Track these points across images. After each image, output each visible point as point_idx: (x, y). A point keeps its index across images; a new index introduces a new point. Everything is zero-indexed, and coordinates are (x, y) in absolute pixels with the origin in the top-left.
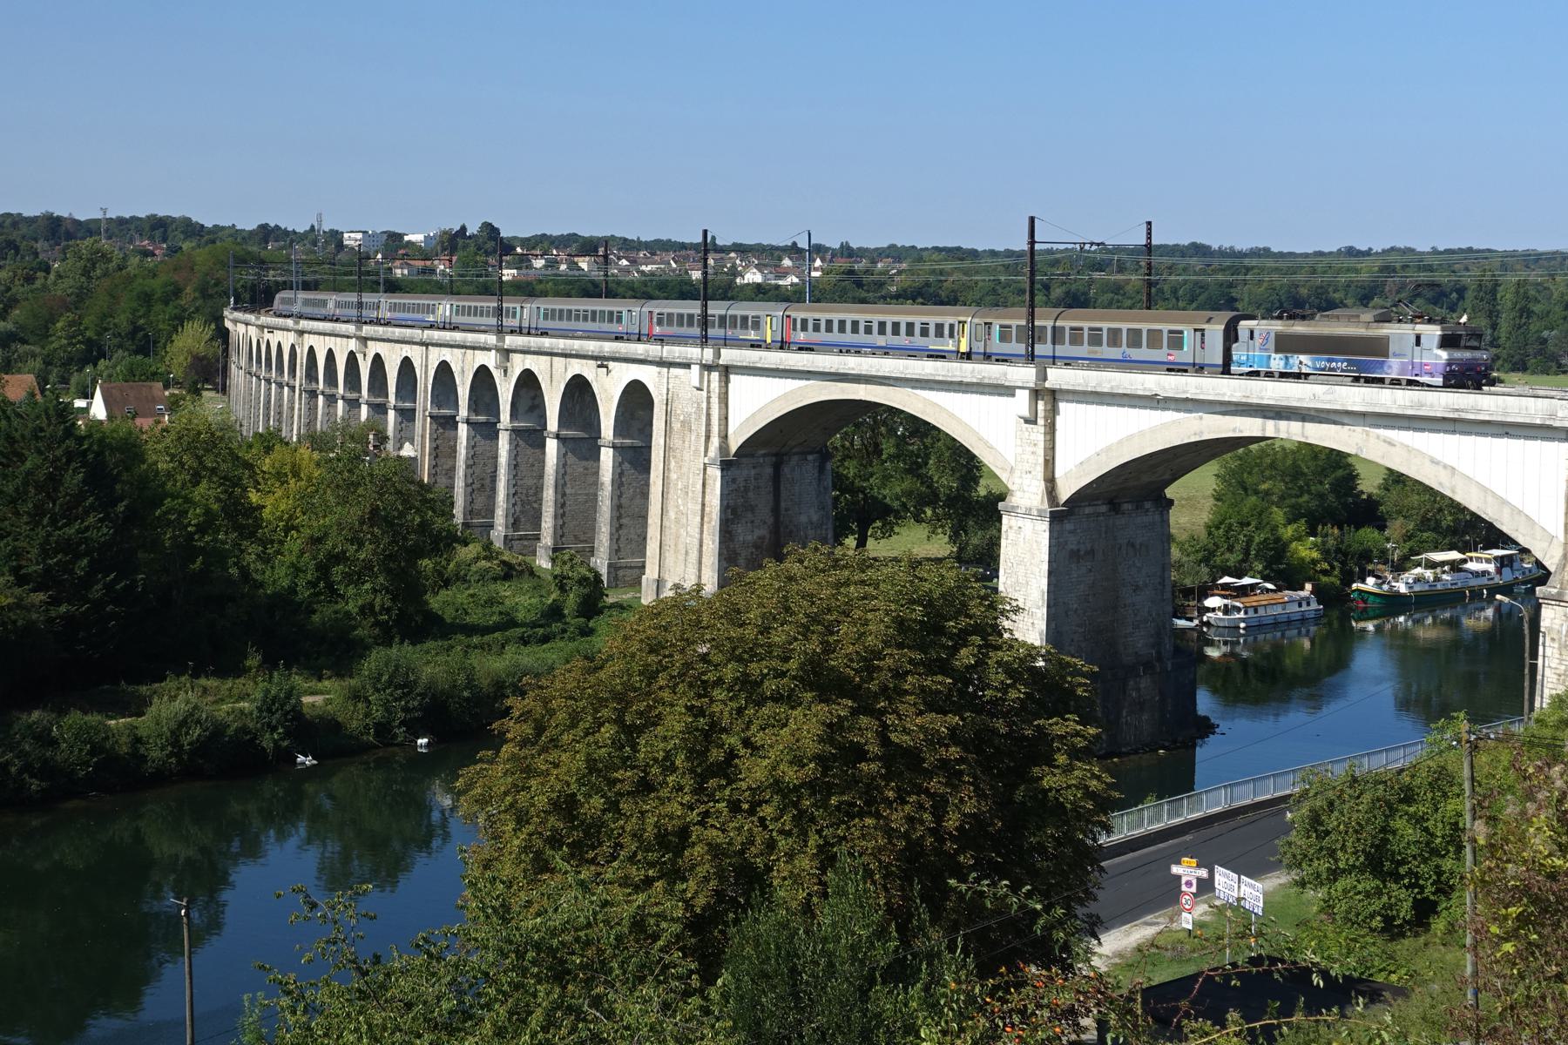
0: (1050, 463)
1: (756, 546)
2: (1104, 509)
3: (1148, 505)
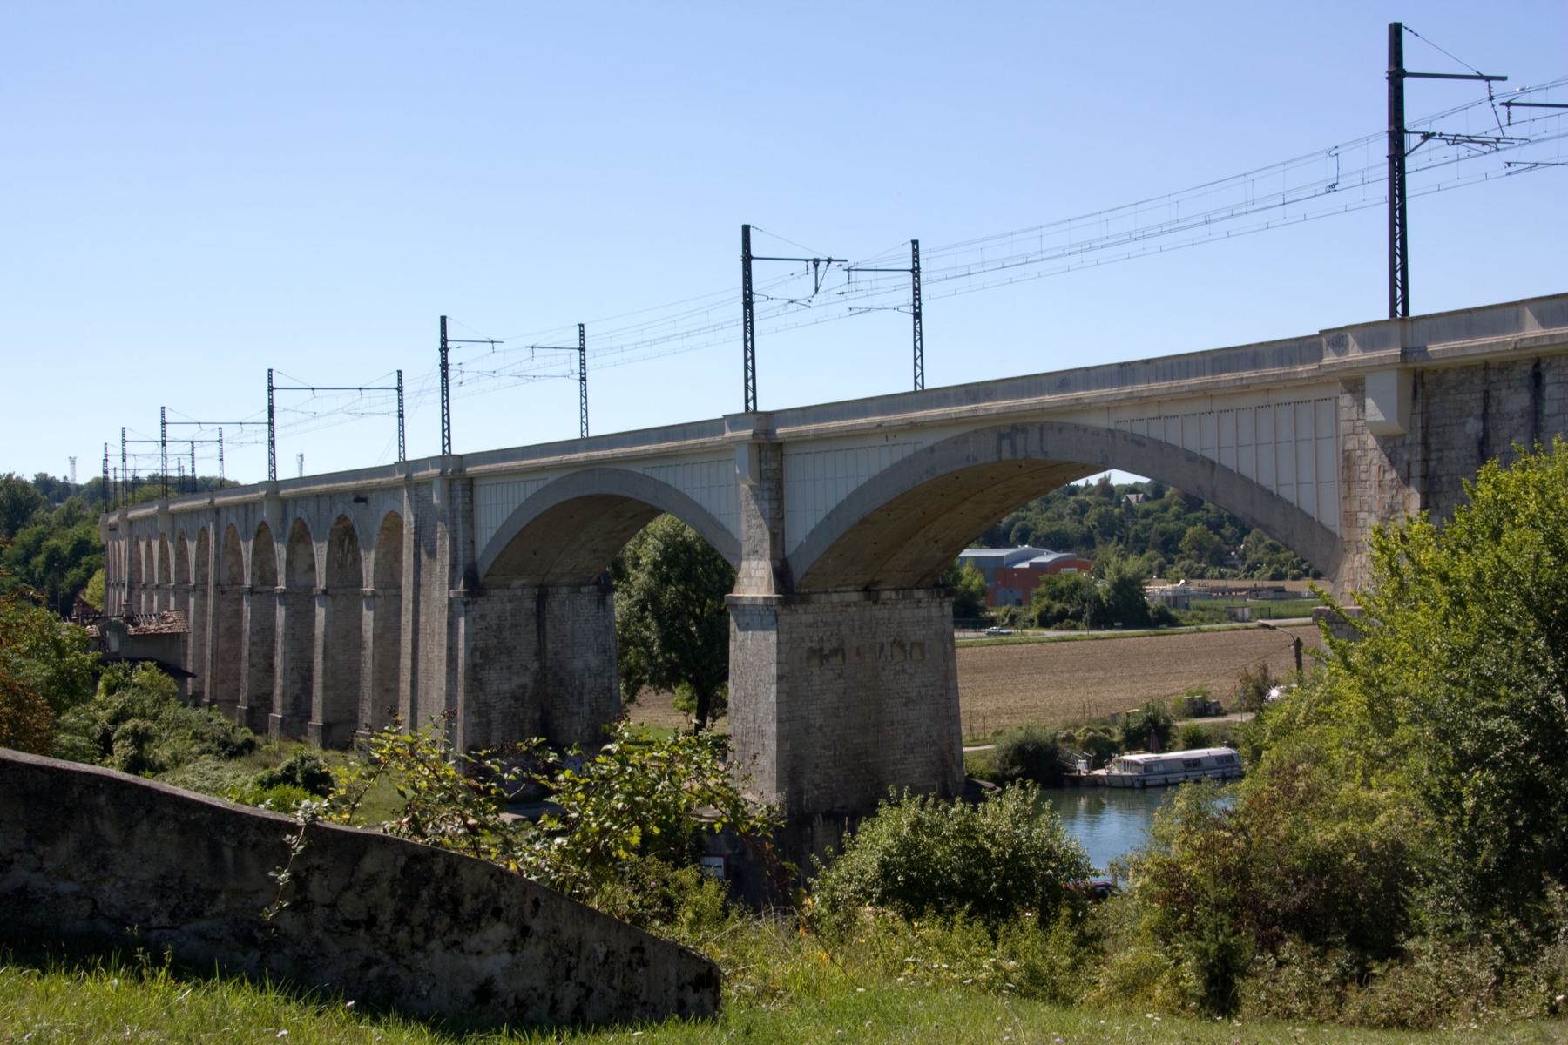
0: (778, 538)
2: (855, 597)
3: (919, 594)
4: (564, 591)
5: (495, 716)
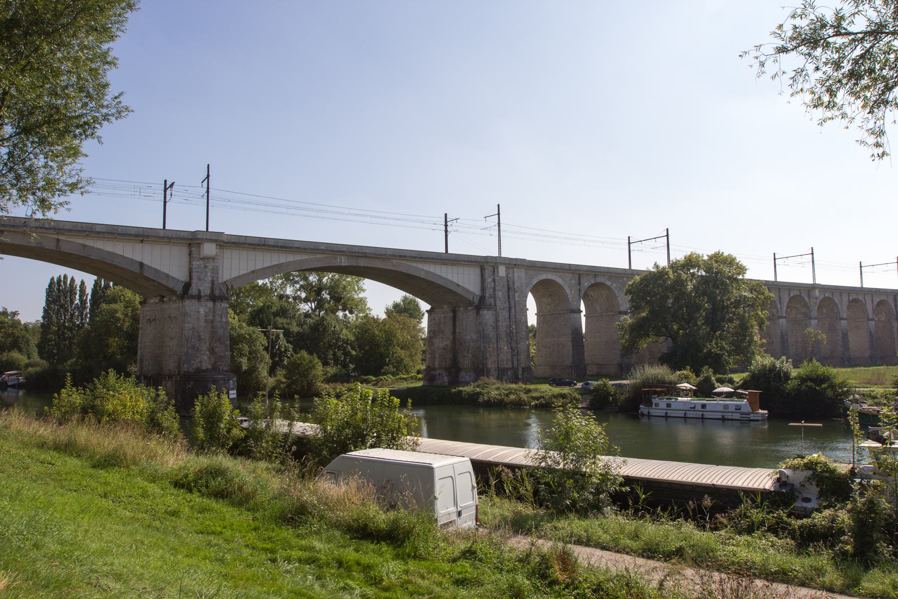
1: (444, 349)
4: (461, 309)
5: (437, 355)
